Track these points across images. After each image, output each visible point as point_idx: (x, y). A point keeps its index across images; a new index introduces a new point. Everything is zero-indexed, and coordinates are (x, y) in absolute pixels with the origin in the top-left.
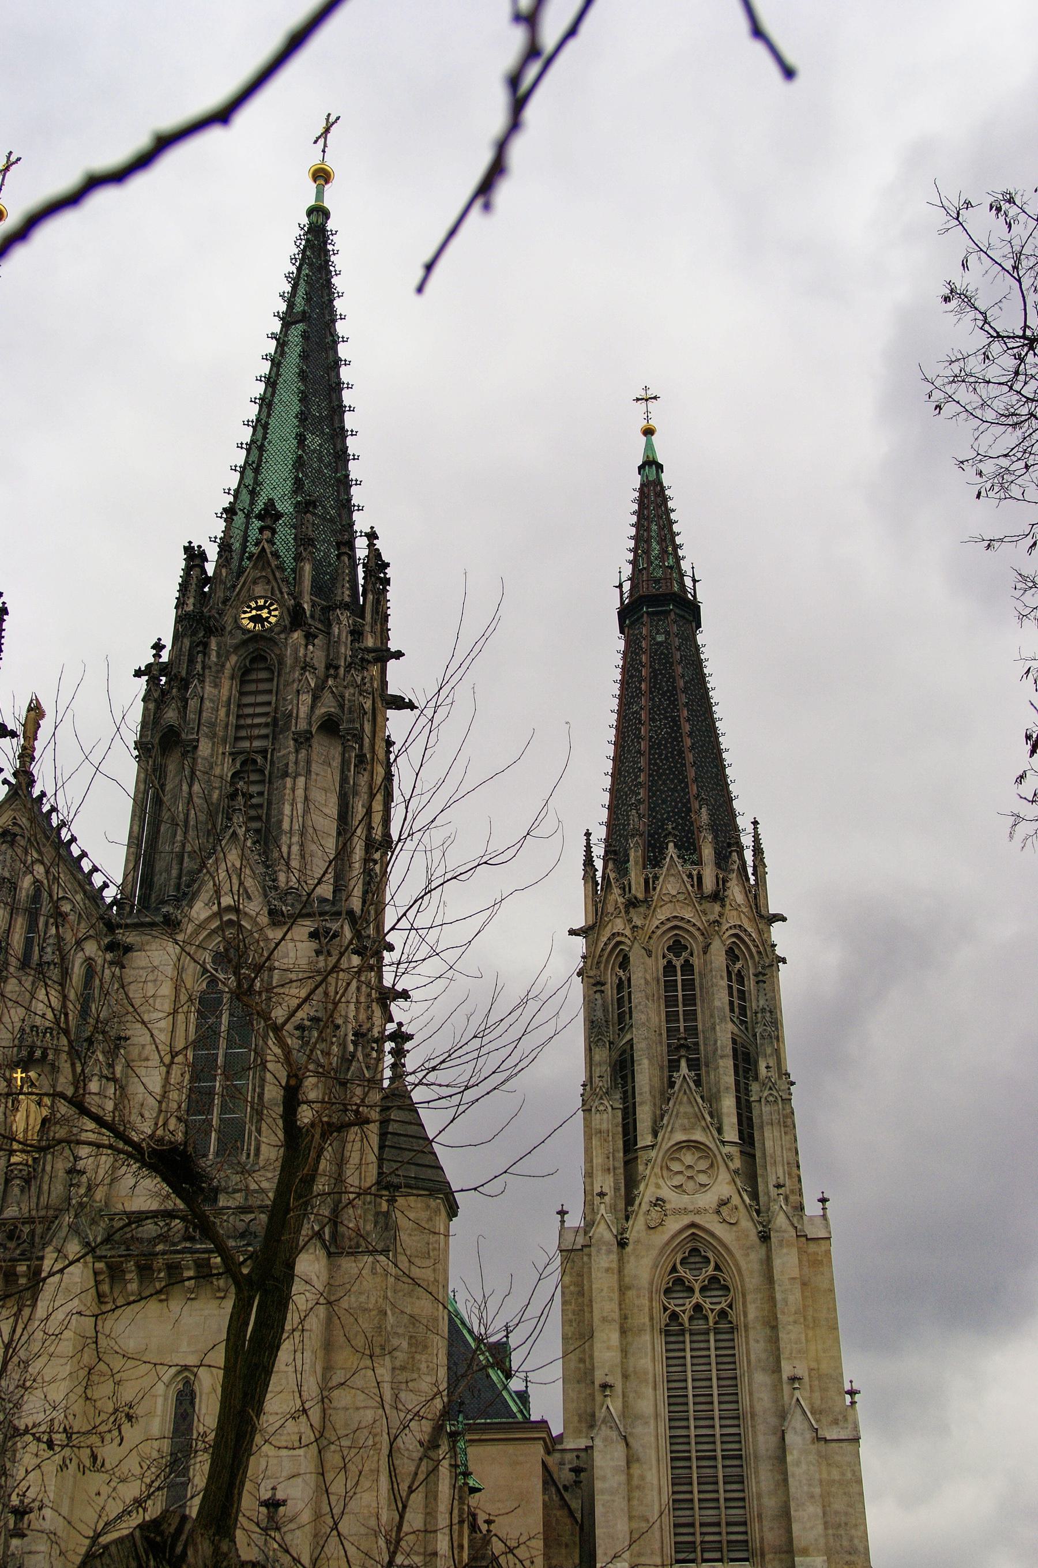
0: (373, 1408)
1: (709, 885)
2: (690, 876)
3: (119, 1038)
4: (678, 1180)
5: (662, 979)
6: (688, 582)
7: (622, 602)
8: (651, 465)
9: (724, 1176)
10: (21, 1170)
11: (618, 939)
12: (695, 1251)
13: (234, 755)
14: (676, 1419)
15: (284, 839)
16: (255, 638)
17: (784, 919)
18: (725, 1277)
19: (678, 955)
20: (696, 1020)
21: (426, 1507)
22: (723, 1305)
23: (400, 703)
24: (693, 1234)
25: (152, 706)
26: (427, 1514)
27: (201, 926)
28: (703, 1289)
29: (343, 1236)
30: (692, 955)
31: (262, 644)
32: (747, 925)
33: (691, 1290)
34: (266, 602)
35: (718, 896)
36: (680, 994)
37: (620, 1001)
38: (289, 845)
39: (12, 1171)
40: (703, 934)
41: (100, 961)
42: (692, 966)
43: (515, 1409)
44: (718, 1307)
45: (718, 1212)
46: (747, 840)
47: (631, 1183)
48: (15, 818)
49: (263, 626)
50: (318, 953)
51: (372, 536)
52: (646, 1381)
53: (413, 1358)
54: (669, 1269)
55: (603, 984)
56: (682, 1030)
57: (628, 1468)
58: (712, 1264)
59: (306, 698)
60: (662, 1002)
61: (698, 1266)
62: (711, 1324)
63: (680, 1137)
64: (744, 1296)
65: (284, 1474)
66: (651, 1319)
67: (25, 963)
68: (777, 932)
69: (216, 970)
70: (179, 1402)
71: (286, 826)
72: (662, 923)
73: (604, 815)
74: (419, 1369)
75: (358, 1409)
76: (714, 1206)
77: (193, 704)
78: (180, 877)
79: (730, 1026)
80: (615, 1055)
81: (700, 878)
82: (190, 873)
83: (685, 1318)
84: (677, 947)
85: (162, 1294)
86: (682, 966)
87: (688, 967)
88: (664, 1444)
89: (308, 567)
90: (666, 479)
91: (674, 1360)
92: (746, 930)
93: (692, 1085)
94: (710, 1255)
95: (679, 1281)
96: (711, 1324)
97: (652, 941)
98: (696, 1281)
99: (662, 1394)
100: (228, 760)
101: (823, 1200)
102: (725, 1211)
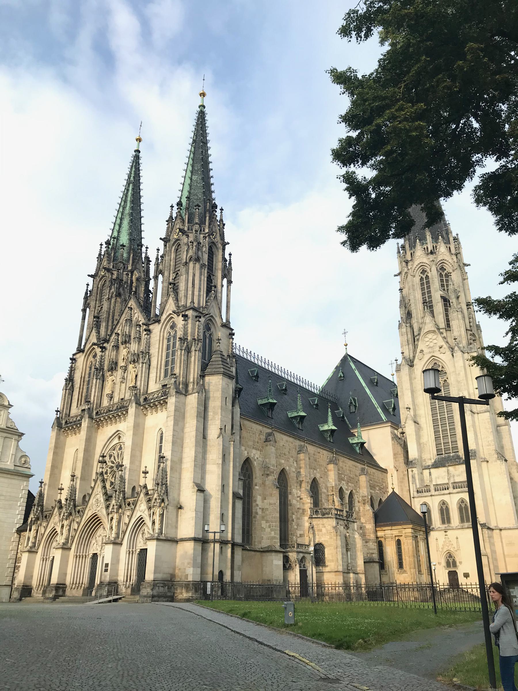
1: (430, 248)
2: (424, 248)
4: (428, 343)
9: (441, 338)
19: (424, 274)
27: (165, 320)
31: (179, 241)
32: (446, 258)
38: (182, 294)
43: (384, 419)
47: (415, 347)
58: (441, 367)
59: (185, 253)
63: (426, 331)
71: (181, 289)
76: (438, 348)
81: (427, 248)
84: (424, 272)
87: (427, 277)
89: (187, 216)
94: (440, 364)
97: (415, 272)
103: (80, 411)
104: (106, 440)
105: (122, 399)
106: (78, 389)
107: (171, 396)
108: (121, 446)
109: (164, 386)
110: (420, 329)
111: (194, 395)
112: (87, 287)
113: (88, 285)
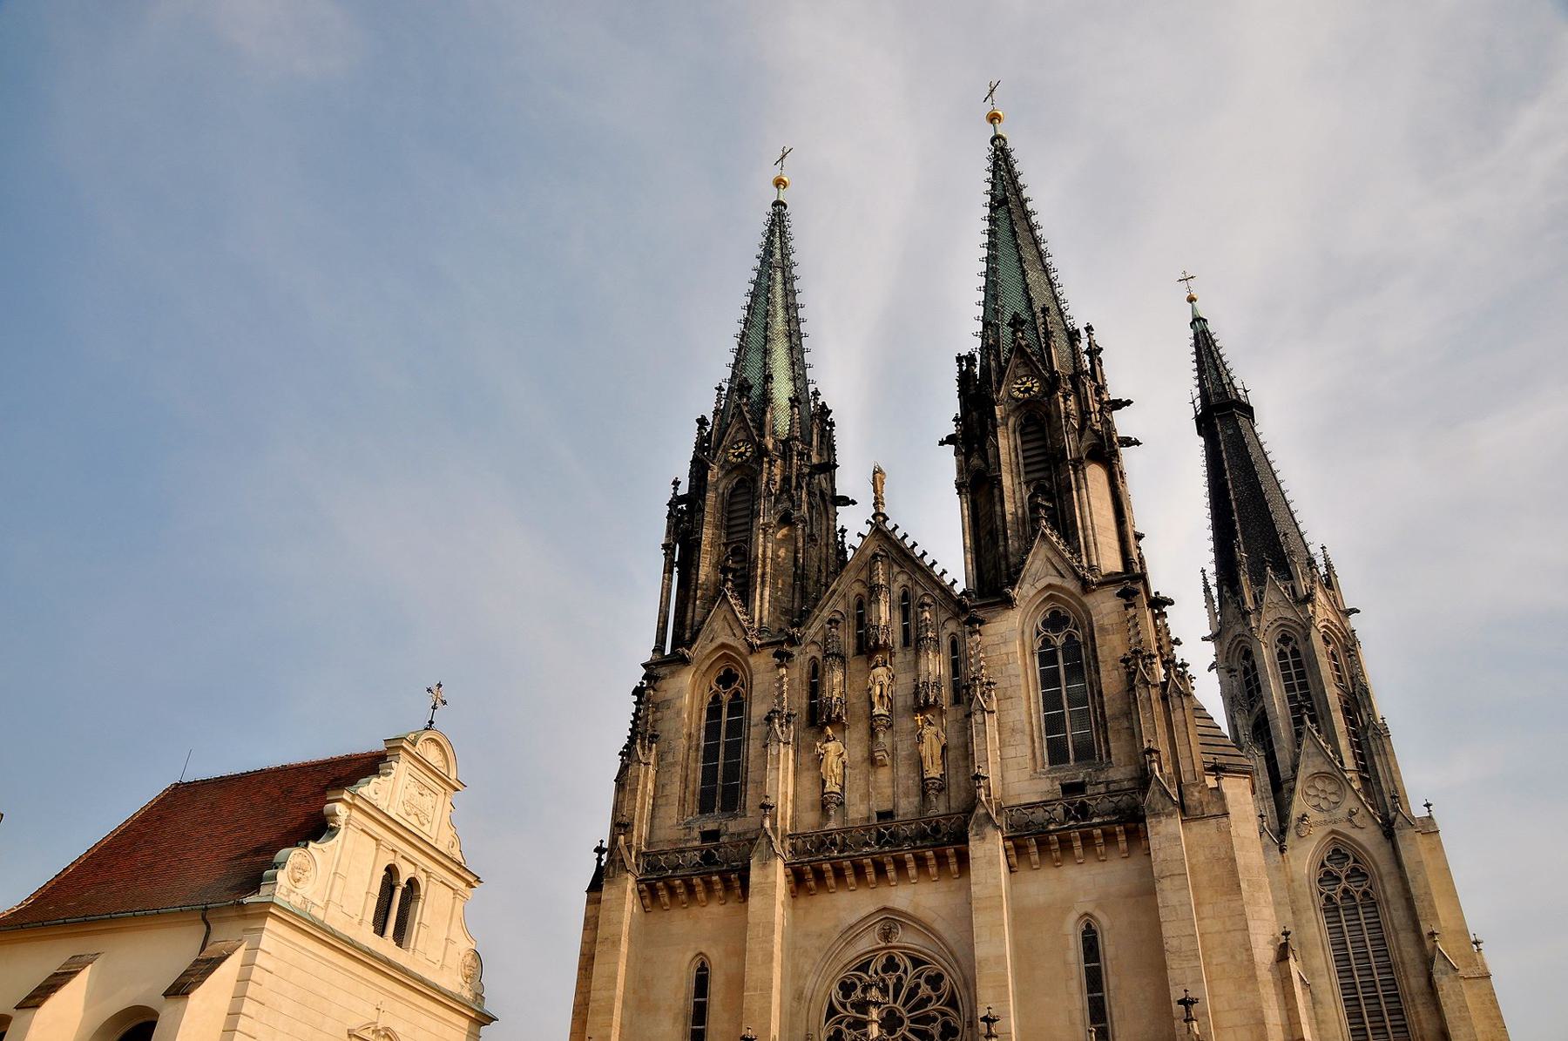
0: (1241, 930)
2: (1286, 588)
3: (989, 683)
4: (1315, 801)
5: (1278, 662)
6: (1241, 392)
7: (1196, 412)
8: (1197, 320)
10: (934, 783)
11: (1240, 639)
12: (1336, 851)
13: (1028, 483)
14: (1345, 971)
15: (1080, 533)
16: (1026, 402)
17: (1358, 611)
18: (1362, 868)
19: (1286, 644)
20: (1308, 688)
21: (1287, 1004)
22: (1365, 887)
23: (1128, 442)
24: (1334, 838)
25: (962, 458)
26: (1288, 1010)
28: (1347, 877)
29: (1189, 807)
30: (1296, 643)
32: (1332, 618)
33: (1338, 879)
34: (1028, 379)
35: (1309, 598)
36: (1293, 671)
37: (1248, 683)
39: (927, 785)
40: (1303, 627)
41: (959, 633)
42: (1298, 651)
44: (1361, 889)
45: (1351, 821)
46: (1320, 561)
48: (879, 546)
49: (1030, 394)
50: (1126, 607)
51: (1089, 329)
52: (1317, 945)
53: (1253, 895)
54: (1320, 864)
55: (1235, 671)
56: (1299, 696)
57: (1314, 1008)
58: (1352, 859)
60: (1281, 677)
61: (1340, 861)
62: (1358, 901)
63: (1312, 770)
64: (1382, 880)
65: (1189, 980)
66: (1313, 901)
67: (906, 643)
68: (1354, 621)
69: (1047, 631)
70: (1085, 940)
72: (1271, 623)
73: (1212, 556)
74: (1259, 903)
75: (1229, 931)
76: (1347, 815)
77: (990, 452)
78: (1008, 568)
79: (1336, 691)
80: (1253, 718)
81: (1293, 588)
82: (1015, 566)
83: (1338, 899)
84: (1284, 639)
85: (1057, 863)
86: (1290, 652)
87: (1295, 652)
88: (1337, 990)
90: (1211, 327)
91: (1335, 930)
92: (1332, 622)
93: (1315, 732)
95: (1328, 873)
96: (1358, 901)
98: (1341, 871)
99: (1329, 949)
100: (1024, 487)
101: (1428, 805)
102: (1355, 819)
103: (696, 833)
104: (836, 936)
105: (883, 816)
106: (678, 768)
107: (1157, 815)
108: (891, 959)
109: (1070, 789)
110: (1295, 768)
111: (1213, 821)
112: (676, 489)
113: (676, 483)
